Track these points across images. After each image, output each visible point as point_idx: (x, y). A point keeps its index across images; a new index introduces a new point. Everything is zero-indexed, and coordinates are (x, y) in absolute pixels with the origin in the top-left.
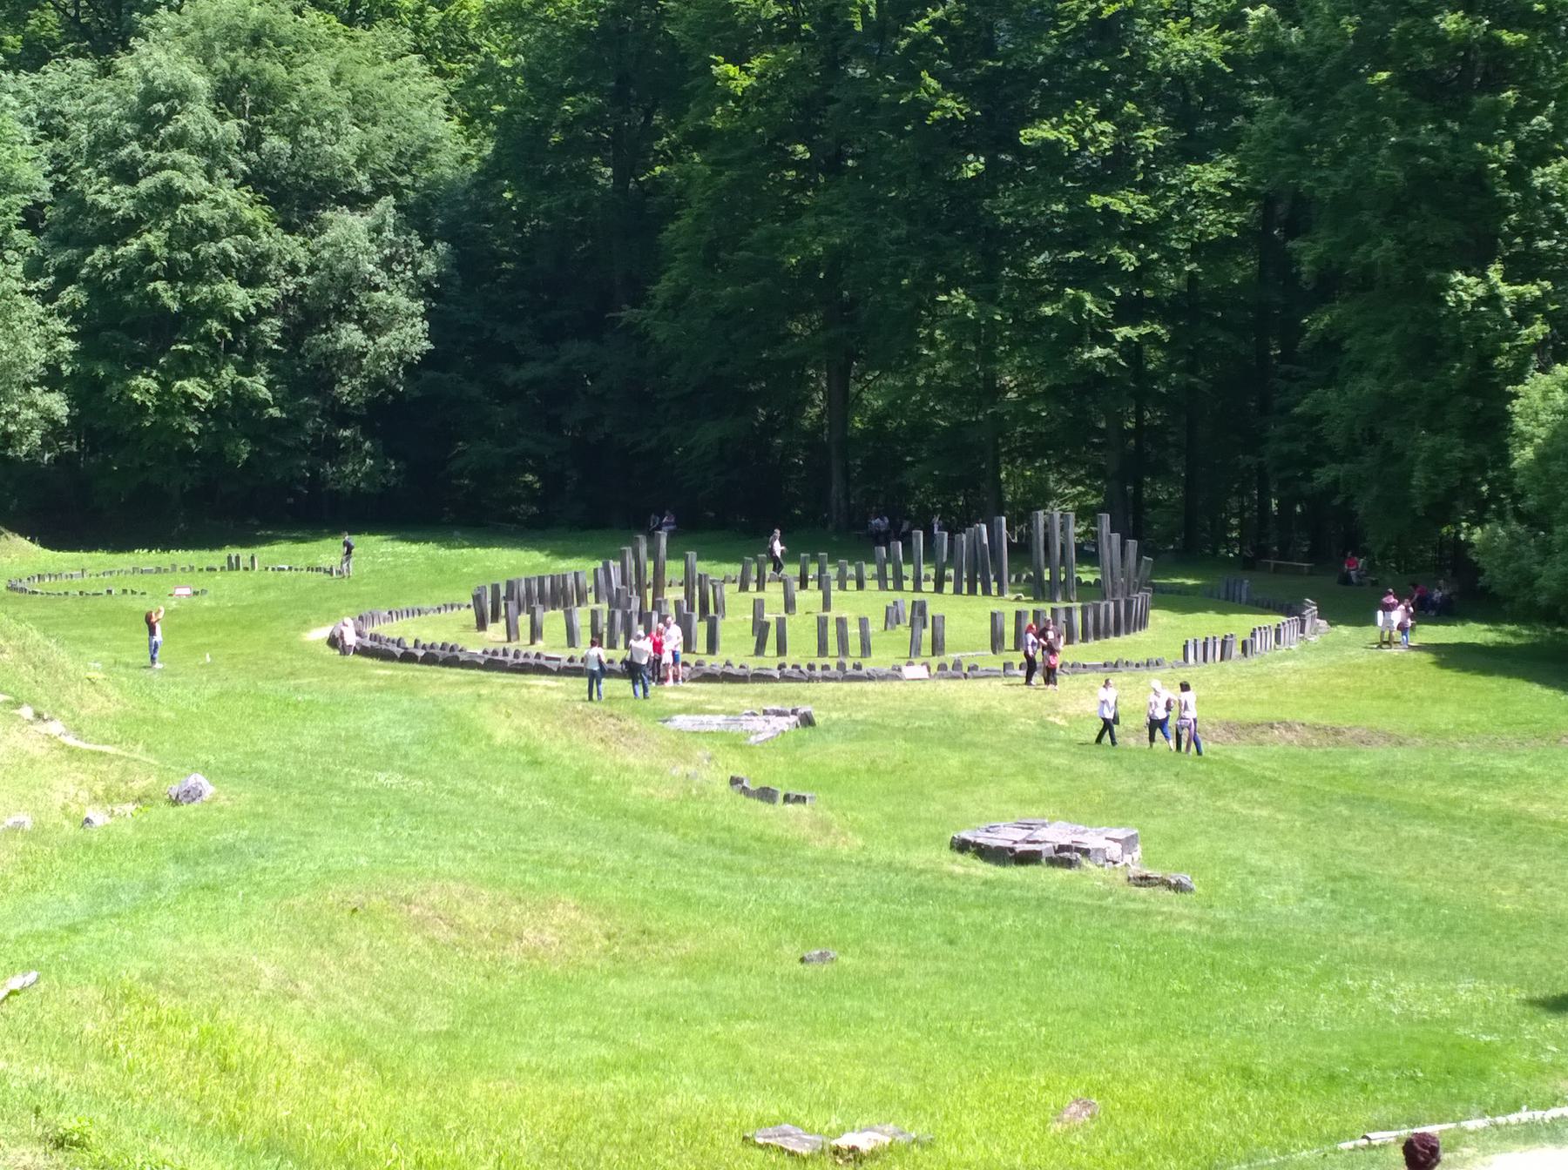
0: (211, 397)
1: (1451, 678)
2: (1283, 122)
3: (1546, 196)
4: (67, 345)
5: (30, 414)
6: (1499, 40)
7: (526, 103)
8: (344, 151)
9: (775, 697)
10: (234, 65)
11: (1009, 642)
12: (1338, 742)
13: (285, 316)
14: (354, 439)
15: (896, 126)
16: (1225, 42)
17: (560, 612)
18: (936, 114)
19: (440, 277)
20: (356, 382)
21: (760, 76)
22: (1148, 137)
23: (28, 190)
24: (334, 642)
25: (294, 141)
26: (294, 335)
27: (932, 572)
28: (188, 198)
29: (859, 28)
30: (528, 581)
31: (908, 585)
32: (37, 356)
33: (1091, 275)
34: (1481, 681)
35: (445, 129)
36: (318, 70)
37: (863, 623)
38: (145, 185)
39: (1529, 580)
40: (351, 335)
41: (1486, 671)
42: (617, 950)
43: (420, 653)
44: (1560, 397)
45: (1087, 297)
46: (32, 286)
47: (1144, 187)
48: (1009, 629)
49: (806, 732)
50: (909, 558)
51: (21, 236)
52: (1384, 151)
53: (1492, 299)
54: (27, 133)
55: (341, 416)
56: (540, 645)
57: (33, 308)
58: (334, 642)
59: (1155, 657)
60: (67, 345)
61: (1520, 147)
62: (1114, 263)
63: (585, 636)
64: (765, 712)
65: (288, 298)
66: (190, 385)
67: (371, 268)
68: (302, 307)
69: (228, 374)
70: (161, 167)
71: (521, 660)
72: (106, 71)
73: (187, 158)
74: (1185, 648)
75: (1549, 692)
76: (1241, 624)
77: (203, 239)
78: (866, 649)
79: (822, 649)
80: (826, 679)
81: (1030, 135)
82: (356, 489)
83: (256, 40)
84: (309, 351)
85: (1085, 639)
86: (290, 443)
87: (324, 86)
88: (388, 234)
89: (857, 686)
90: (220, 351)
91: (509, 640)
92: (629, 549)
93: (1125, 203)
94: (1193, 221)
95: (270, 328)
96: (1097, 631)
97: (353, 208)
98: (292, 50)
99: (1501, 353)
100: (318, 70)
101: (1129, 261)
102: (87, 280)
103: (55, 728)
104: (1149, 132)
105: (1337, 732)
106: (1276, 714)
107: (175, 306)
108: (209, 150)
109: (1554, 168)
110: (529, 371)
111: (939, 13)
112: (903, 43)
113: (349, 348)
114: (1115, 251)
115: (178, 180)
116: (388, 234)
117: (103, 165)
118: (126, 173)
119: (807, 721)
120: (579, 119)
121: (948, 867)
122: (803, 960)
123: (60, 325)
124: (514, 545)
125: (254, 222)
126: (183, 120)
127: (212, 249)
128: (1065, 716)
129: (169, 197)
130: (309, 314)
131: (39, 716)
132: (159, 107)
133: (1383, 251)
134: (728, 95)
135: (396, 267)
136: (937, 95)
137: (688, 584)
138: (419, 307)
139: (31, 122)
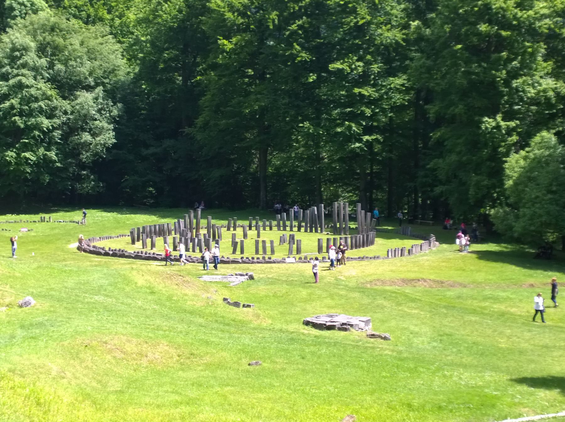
0: (34, 159)
1: (483, 263)
2: (424, 63)
3: (517, 90)
6: (500, 35)
7: (150, 53)
9: (239, 269)
10: (44, 39)
11: (324, 250)
12: (442, 286)
13: (62, 130)
14: (87, 175)
15: (285, 63)
16: (403, 34)
17: (162, 238)
18: (299, 59)
19: (119, 116)
20: (88, 154)
21: (236, 44)
22: (375, 68)
26: (65, 137)
27: (297, 224)
28: (27, 87)
29: (271, 27)
30: (150, 226)
31: (288, 228)
33: (354, 117)
35: (122, 62)
36: (75, 41)
37: (272, 242)
38: (11, 82)
39: (511, 228)
40: (86, 137)
41: (496, 261)
42: (182, 361)
43: (111, 253)
44: (522, 163)
45: (353, 125)
47: (374, 86)
48: (324, 245)
49: (251, 282)
50: (288, 219)
52: (460, 74)
53: (498, 127)
55: (82, 166)
56: (155, 250)
59: (377, 255)
61: (508, 73)
62: (363, 113)
64: (236, 275)
65: (63, 123)
66: (27, 155)
67: (94, 112)
68: (69, 127)
69: (41, 151)
70: (18, 75)
71: (148, 255)
74: (388, 252)
75: (518, 268)
76: (408, 243)
77: (33, 101)
78: (273, 252)
79: (257, 252)
80: (258, 263)
82: (88, 193)
83: (53, 29)
84: (71, 142)
85: (352, 248)
86: (64, 176)
87: (77, 46)
88: (100, 100)
89: (269, 265)
90: (39, 142)
91: (143, 248)
92: (187, 215)
93: (367, 91)
94: (391, 98)
95: (57, 134)
96: (356, 246)
97: (87, 91)
98: (65, 33)
99: (501, 146)
100: (75, 41)
101: (368, 112)
104: (376, 66)
105: (442, 283)
107: (22, 126)
108: (35, 69)
109: (520, 80)
110: (152, 150)
111: (300, 22)
112: (287, 33)
113: (86, 141)
114: (363, 108)
115: (24, 80)
116: (100, 100)
119: (251, 278)
120: (170, 59)
121: (302, 331)
122: (249, 365)
124: (145, 214)
125: (51, 95)
126: (25, 58)
127: (36, 105)
128: (345, 276)
129: (20, 86)
132: (17, 53)
133: (459, 109)
134: (224, 51)
135: (103, 112)
136: (299, 52)
137: (208, 228)
138: (111, 126)
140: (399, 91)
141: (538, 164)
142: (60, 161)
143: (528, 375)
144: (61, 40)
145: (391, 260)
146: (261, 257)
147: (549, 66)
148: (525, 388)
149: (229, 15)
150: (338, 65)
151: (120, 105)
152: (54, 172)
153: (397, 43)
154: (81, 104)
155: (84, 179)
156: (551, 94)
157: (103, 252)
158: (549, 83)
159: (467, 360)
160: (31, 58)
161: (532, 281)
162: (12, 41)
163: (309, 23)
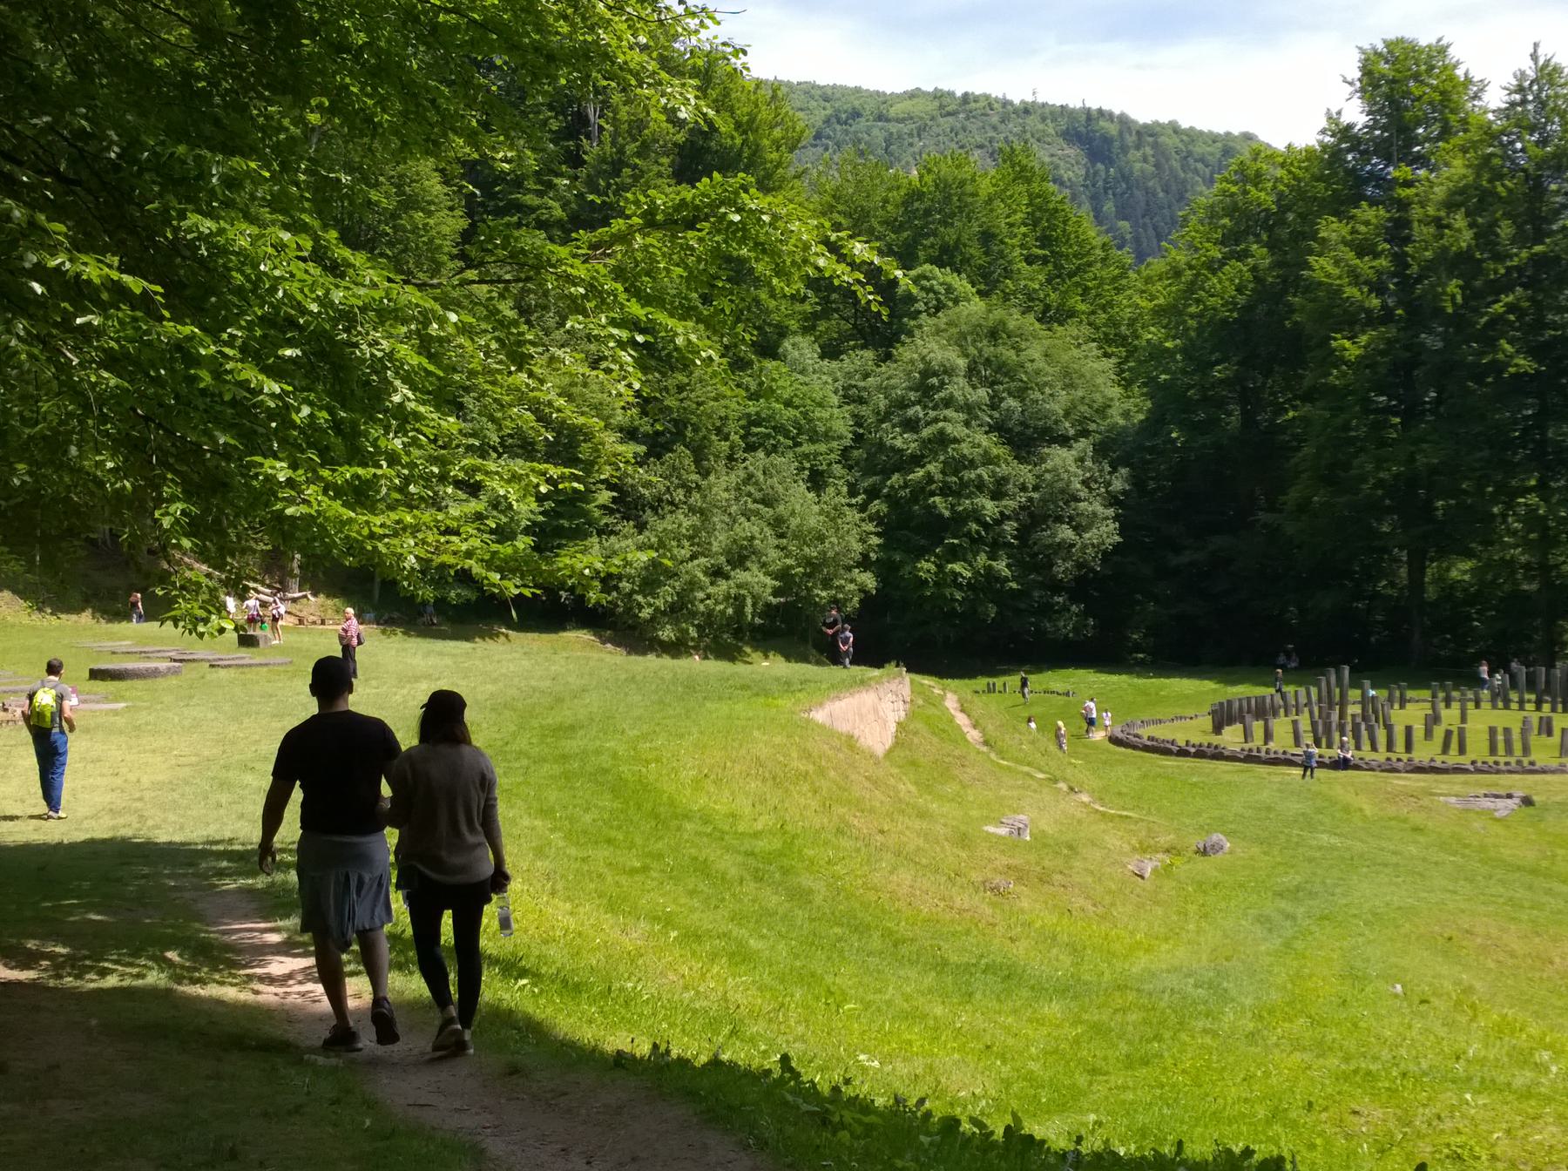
0: (969, 575)
5: (852, 587)
7: (1184, 372)
8: (1057, 407)
9: (1478, 784)
10: (980, 351)
13: (1017, 520)
15: (1479, 379)
17: (1261, 723)
18: (1512, 370)
19: (1124, 492)
20: (1069, 565)
23: (840, 437)
25: (1022, 401)
26: (1023, 533)
27: (1533, 697)
28: (956, 441)
31: (1514, 706)
32: (858, 547)
36: (1034, 351)
38: (926, 432)
40: (1065, 533)
46: (854, 501)
49: (1530, 810)
51: (838, 469)
54: (835, 400)
55: (1056, 587)
56: (1271, 745)
57: (853, 515)
60: (875, 540)
63: (1308, 739)
66: (957, 567)
68: (1031, 515)
69: (982, 559)
70: (936, 420)
72: (888, 357)
73: (955, 415)
77: (965, 468)
79: (1493, 750)
80: (1510, 772)
83: (994, 335)
86: (1022, 606)
90: (976, 541)
95: (1010, 527)
100: (1034, 351)
102: (888, 496)
103: (1085, 798)
107: (947, 514)
108: (968, 408)
110: (1185, 558)
111: (1511, 298)
115: (949, 429)
116: (1089, 463)
117: (896, 420)
118: (911, 425)
119: (1527, 801)
120: (1221, 381)
123: (870, 527)
124: (1190, 675)
125: (998, 457)
129: (943, 440)
130: (1033, 519)
131: (1072, 789)
132: (934, 381)
136: (1511, 357)
137: (1364, 701)
138: (1111, 512)
139: (836, 392)
142: (1014, 579)
144: (1012, 353)
146: (1502, 760)
149: (1351, 292)
151: (1124, 471)
154: (1054, 470)
155: (1056, 612)
157: (1175, 749)
160: (959, 388)
162: (923, 359)
163: (1529, 299)
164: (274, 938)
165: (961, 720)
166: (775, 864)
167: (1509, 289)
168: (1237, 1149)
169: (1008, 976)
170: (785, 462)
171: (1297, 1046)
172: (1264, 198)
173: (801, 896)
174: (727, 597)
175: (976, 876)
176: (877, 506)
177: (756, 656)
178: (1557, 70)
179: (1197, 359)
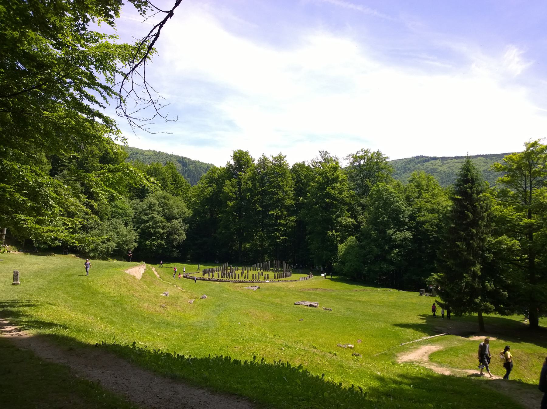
1: (334, 283)
4: (138, 237)
8: (176, 212)
15: (253, 211)
22: (285, 213)
24: (184, 277)
26: (168, 236)
32: (134, 238)
33: (277, 230)
34: (340, 283)
36: (172, 201)
37: (239, 275)
38: (150, 216)
40: (176, 236)
44: (345, 247)
50: (257, 266)
51: (131, 223)
53: (333, 235)
55: (174, 247)
58: (184, 277)
60: (138, 237)
63: (220, 276)
66: (154, 242)
72: (142, 201)
76: (305, 275)
79: (253, 278)
81: (270, 213)
83: (164, 198)
87: (173, 204)
90: (158, 238)
95: (165, 235)
98: (169, 199)
100: (172, 201)
101: (283, 229)
103: (179, 288)
106: (318, 287)
108: (158, 211)
115: (154, 215)
118: (147, 214)
119: (259, 288)
129: (153, 218)
130: (170, 233)
137: (231, 269)
140: (293, 221)
141: (351, 247)
143: (398, 323)
145: (301, 282)
147: (348, 214)
148: (398, 328)
149: (231, 194)
150: (272, 212)
151: (188, 225)
152: (164, 249)
153: (292, 205)
156: (350, 223)
158: (349, 220)
159: (367, 318)
161: (356, 289)
164: (6, 322)
165: (156, 273)
166: (119, 303)
167: (258, 195)
168: (219, 355)
169: (168, 324)
170: (120, 221)
171: (224, 335)
172: (216, 176)
173: (124, 309)
174: (106, 247)
175: (159, 304)
176: (139, 230)
177: (111, 260)
178: (267, 158)
179: (203, 204)
